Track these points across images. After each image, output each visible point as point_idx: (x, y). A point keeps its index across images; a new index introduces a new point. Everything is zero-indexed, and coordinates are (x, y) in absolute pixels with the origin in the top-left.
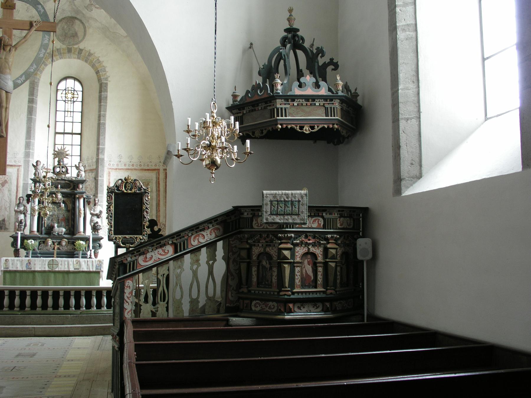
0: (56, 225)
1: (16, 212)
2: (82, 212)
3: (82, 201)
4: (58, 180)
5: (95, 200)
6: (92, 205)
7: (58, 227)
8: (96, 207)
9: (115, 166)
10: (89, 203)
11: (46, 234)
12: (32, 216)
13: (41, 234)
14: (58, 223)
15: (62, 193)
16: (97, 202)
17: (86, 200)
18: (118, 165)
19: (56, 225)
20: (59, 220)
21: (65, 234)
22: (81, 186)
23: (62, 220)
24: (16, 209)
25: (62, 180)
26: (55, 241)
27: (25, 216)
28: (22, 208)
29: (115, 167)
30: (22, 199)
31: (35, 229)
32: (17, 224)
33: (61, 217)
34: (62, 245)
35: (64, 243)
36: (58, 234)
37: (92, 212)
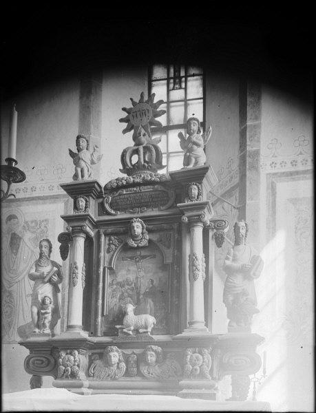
0: (130, 308)
1: (32, 277)
2: (200, 263)
3: (198, 231)
4: (135, 185)
5: (236, 228)
6: (228, 242)
7: (137, 312)
8: (241, 247)
9: (289, 165)
10: (219, 241)
11: (105, 334)
12: (72, 283)
13: (94, 334)
14: (137, 303)
15: (146, 220)
16: (243, 232)
17: (211, 234)
18: (294, 163)
19: (130, 308)
20: (138, 294)
21: (154, 331)
22: (195, 191)
23: (146, 294)
24: (33, 271)
25: (146, 183)
26: (128, 352)
27: (56, 290)
28: (46, 269)
29: (289, 168)
30: (45, 244)
31: (77, 318)
32: (35, 310)
33: (145, 285)
34: (147, 364)
35: (151, 357)
36: (136, 331)
37: (228, 263)
